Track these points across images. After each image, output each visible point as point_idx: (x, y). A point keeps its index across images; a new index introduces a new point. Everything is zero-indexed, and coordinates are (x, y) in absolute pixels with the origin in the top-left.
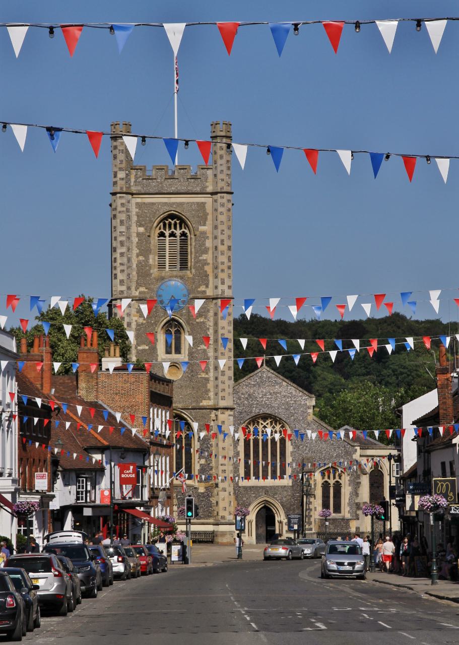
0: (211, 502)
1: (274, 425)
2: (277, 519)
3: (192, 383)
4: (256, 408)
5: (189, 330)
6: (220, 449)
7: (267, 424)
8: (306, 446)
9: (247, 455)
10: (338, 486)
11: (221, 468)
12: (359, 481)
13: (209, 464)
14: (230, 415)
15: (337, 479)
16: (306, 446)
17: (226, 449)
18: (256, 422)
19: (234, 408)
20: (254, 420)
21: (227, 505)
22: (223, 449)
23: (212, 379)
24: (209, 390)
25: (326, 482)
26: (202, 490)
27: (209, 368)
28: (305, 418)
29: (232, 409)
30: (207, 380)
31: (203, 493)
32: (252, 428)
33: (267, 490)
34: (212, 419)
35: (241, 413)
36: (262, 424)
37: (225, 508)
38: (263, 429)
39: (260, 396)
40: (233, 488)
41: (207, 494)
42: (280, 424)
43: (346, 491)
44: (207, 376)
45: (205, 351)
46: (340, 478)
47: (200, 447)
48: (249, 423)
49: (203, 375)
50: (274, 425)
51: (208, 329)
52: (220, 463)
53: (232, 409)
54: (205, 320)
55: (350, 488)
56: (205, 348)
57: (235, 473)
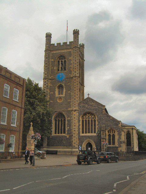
10: (114, 136)
11: (74, 129)
20: (85, 114)
29: (78, 111)
30: (70, 102)
32: (84, 117)
33: (89, 137)
43: (117, 137)
46: (115, 133)
53: (78, 111)
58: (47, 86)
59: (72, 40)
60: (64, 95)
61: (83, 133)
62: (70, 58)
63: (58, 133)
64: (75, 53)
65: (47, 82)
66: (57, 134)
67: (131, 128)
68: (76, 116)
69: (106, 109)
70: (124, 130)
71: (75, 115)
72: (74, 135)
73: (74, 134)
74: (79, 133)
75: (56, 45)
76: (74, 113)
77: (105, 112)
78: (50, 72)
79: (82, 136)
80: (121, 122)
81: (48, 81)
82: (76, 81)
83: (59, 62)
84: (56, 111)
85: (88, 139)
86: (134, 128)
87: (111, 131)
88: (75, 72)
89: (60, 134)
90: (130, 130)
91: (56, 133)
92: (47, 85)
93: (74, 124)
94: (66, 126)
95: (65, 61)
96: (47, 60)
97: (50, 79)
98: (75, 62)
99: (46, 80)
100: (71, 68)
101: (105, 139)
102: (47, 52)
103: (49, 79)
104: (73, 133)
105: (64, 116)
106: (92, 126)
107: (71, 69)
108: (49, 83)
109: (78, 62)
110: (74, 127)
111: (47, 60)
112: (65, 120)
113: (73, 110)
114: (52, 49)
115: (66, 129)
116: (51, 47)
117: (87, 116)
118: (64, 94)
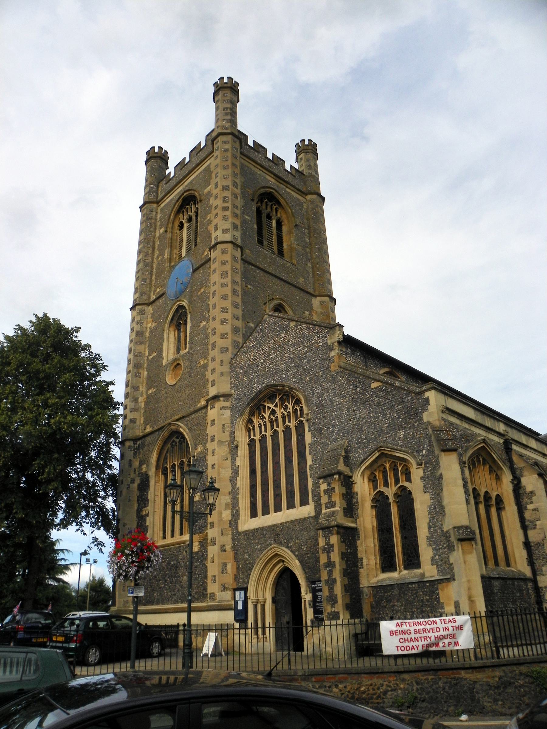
8: (334, 426)
17: (216, 466)
18: (261, 407)
36: (269, 408)
42: (293, 397)
46: (409, 480)
55: (427, 496)
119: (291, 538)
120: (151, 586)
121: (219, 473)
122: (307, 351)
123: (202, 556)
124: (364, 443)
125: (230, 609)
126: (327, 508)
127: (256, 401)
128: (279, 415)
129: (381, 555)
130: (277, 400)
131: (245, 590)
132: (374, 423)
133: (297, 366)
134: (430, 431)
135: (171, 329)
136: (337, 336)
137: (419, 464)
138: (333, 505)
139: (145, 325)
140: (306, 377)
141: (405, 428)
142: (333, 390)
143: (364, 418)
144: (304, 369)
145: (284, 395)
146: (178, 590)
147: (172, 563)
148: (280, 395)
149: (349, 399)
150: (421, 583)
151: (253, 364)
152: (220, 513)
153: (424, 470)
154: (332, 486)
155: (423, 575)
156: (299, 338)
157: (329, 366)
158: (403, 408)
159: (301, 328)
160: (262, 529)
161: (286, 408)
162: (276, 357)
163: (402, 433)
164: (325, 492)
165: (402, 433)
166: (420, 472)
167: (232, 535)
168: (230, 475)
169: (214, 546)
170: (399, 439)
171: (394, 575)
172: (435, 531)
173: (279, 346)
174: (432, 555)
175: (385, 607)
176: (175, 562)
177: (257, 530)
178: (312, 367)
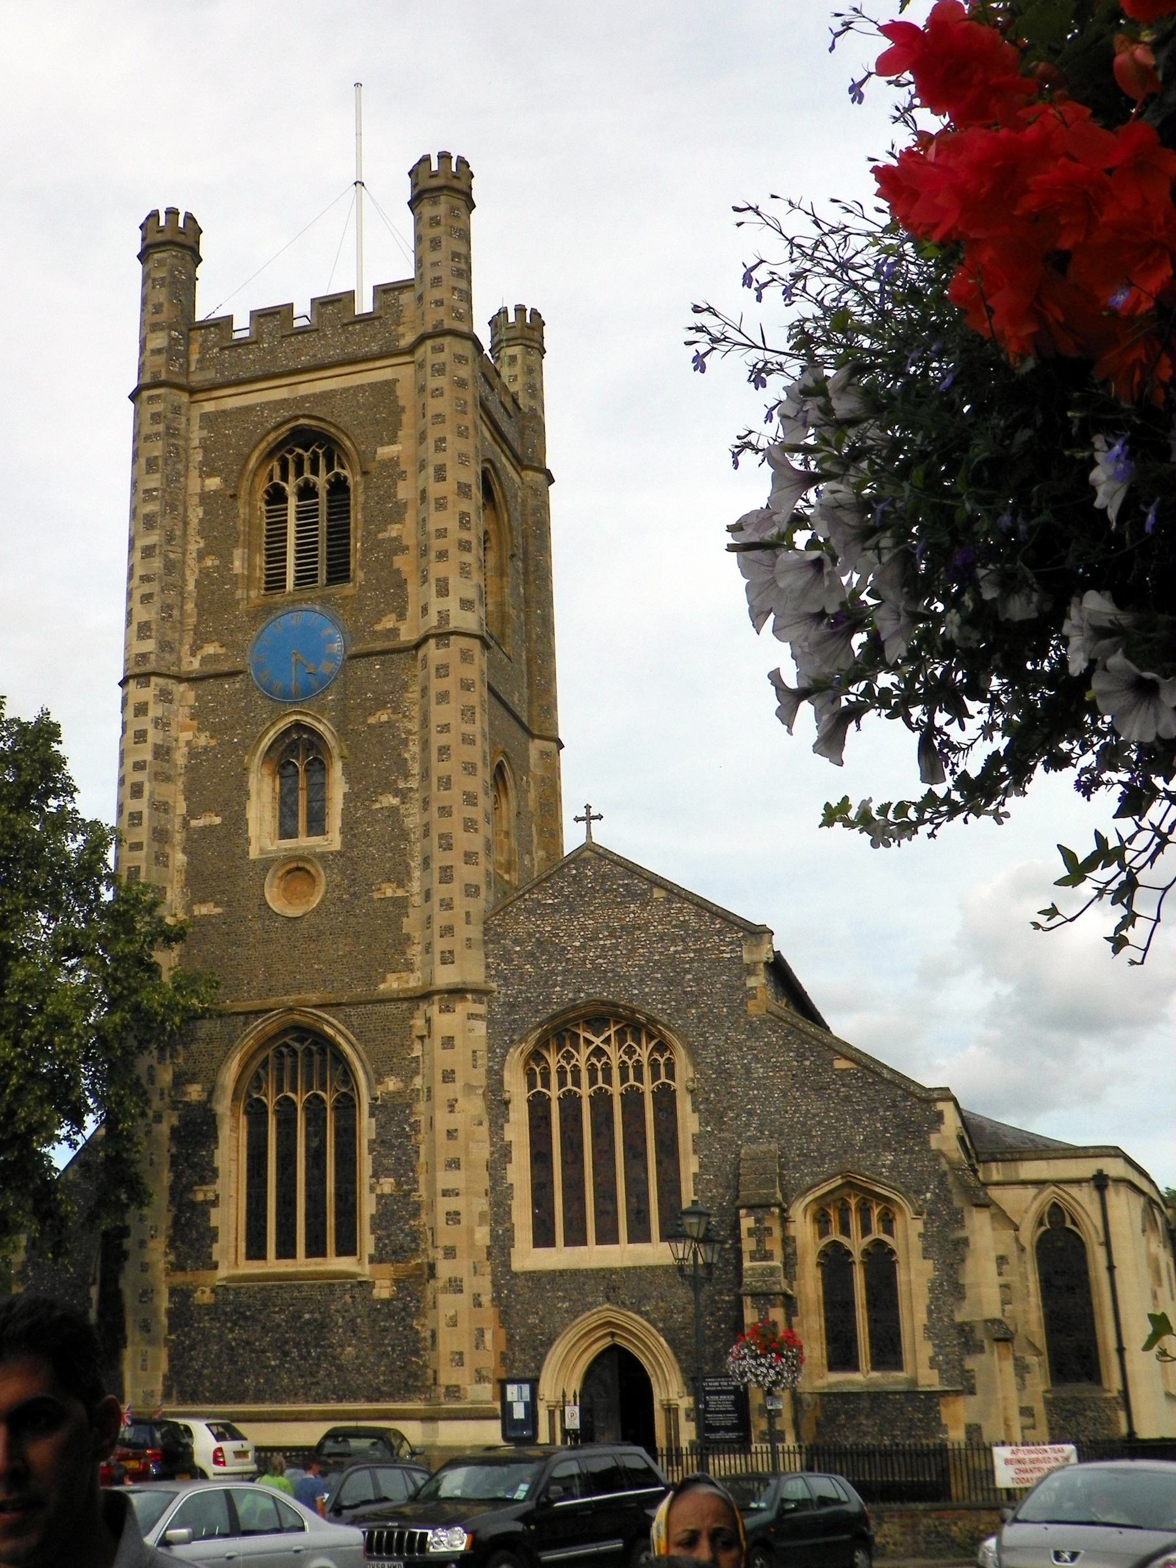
0: (417, 1332)
1: (630, 1042)
2: (659, 1396)
3: (352, 920)
4: (564, 984)
5: (346, 752)
6: (441, 1137)
7: (607, 1041)
8: (750, 1113)
9: (540, 1157)
11: (445, 1205)
12: (961, 1234)
13: (407, 1194)
14: (471, 1016)
15: (877, 1233)
16: (750, 1113)
17: (461, 1135)
19: (488, 992)
21: (466, 1346)
22: (451, 1134)
23: (417, 900)
24: (408, 937)
25: (836, 1244)
26: (384, 1290)
27: (408, 866)
28: (738, 1009)
29: (481, 993)
30: (402, 905)
31: (386, 1302)
32: (553, 1060)
34: (416, 1032)
35: (512, 1007)
36: (588, 1042)
37: (461, 1354)
38: (594, 1060)
39: (577, 944)
40: (488, 1278)
41: (401, 1306)
42: (651, 1037)
44: (400, 893)
45: (394, 810)
46: (889, 1231)
47: (378, 1134)
48: (546, 1046)
49: (389, 891)
50: (630, 1042)
51: (405, 742)
52: (441, 1186)
53: (481, 993)
54: (394, 717)
55: (929, 1264)
56: (395, 801)
57: (496, 1221)
58: (162, 752)
59: (407, 272)
60: (333, 841)
61: (543, 1237)
62: (385, 451)
63: (286, 1250)
64: (438, 393)
65: (155, 711)
66: (273, 1265)
67: (1087, 1168)
68: (457, 1059)
69: (779, 970)
70: (1007, 1198)
71: (448, 1042)
72: (445, 1269)
73: (450, 1253)
74: (501, 1245)
75: (242, 322)
76: (445, 1023)
77: (781, 1006)
78: (190, 606)
79: (536, 1278)
80: (947, 1108)
81: (165, 696)
82: (448, 683)
83: (276, 496)
84: (258, 1013)
85: (607, 1311)
86: (1114, 1168)
87: (844, 1211)
88: (443, 591)
89: (301, 1263)
90: (1074, 1191)
91: (256, 1251)
92: (154, 736)
93: (445, 1150)
94: (365, 1164)
95: (339, 487)
96: (154, 481)
97: (189, 680)
98: (435, 489)
99: (146, 694)
100: (398, 547)
101: (790, 1304)
102: (158, 407)
103: (180, 679)
104: (443, 1241)
105: (340, 1058)
106: (635, 1152)
107: (399, 561)
108: (182, 714)
109: (463, 490)
110: (446, 1179)
111: (154, 481)
112: (347, 1106)
113: (426, 996)
114: (211, 375)
115: (368, 1206)
116: (195, 348)
117: (582, 1057)
118: (335, 821)
119: (647, 1297)
120: (232, 1362)
121: (467, 1151)
122: (692, 960)
123: (404, 1309)
124: (814, 1157)
125: (495, 1418)
126: (753, 1259)
127: (557, 1021)
128: (615, 1064)
129: (828, 1343)
130: (612, 1032)
131: (534, 1383)
132: (835, 1128)
133: (670, 982)
134: (945, 1167)
135: (265, 771)
136: (765, 955)
137: (919, 1213)
138: (768, 1256)
139: (173, 732)
140: (689, 1007)
141: (895, 1150)
142: (750, 1048)
143: (815, 1116)
144: (685, 993)
145: (627, 1026)
146: (329, 1375)
147: (307, 1316)
148: (616, 1023)
149: (787, 1076)
150: (912, 1394)
151: (552, 943)
152: (471, 1232)
153: (925, 1224)
154: (767, 1224)
155: (914, 1381)
156: (675, 927)
157: (743, 1003)
158: (895, 1116)
159: (680, 910)
160: (575, 1273)
161: (630, 1052)
162: (615, 947)
163: (889, 1158)
164: (751, 1232)
165: (889, 1158)
166: (919, 1226)
167: (494, 1274)
168: (487, 1156)
169: (459, 1295)
170: (884, 1166)
171: (857, 1377)
172: (940, 1319)
173: (623, 928)
174: (931, 1354)
175: (844, 1426)
176: (317, 1315)
177: (562, 1273)
178: (705, 993)
